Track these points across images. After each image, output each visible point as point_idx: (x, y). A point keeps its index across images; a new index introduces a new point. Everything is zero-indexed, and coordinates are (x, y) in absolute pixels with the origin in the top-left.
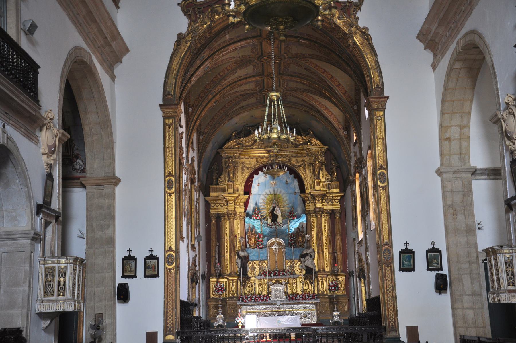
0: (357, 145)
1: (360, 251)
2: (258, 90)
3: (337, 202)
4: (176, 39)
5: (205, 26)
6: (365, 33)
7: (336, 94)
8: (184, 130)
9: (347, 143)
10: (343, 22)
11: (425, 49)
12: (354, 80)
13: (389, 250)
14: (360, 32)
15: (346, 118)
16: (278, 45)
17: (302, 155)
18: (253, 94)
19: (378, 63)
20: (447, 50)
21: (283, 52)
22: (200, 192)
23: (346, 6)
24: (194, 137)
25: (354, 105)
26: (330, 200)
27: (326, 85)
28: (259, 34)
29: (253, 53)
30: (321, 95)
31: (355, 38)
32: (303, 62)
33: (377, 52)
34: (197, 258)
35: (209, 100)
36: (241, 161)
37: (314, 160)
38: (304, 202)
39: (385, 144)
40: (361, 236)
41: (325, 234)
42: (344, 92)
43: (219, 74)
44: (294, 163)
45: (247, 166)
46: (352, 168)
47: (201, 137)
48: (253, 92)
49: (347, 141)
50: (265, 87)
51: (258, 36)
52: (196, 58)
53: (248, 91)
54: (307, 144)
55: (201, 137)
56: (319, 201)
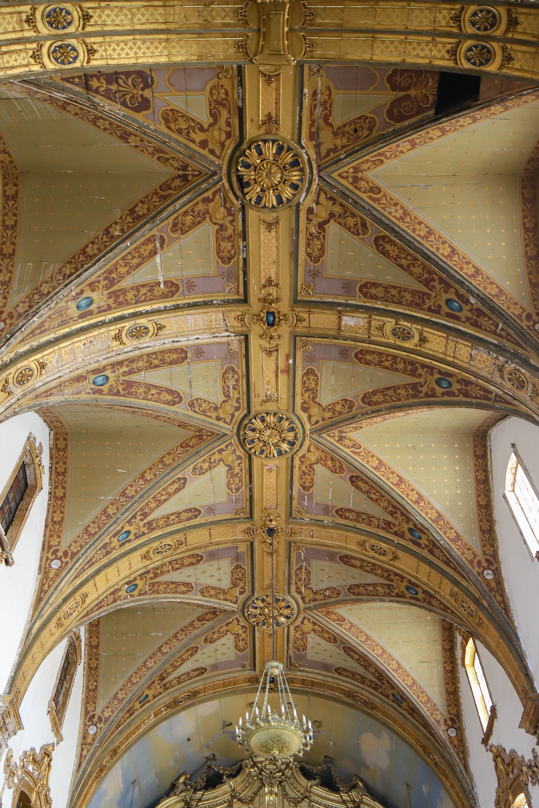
2: (242, 598)
9: (460, 759)
25: (485, 569)
32: (348, 451)
35: (112, 556)
42: (453, 535)
43: (142, 476)
49: (458, 754)
50: (257, 585)
51: (239, 301)
53: (216, 596)
55: (92, 730)
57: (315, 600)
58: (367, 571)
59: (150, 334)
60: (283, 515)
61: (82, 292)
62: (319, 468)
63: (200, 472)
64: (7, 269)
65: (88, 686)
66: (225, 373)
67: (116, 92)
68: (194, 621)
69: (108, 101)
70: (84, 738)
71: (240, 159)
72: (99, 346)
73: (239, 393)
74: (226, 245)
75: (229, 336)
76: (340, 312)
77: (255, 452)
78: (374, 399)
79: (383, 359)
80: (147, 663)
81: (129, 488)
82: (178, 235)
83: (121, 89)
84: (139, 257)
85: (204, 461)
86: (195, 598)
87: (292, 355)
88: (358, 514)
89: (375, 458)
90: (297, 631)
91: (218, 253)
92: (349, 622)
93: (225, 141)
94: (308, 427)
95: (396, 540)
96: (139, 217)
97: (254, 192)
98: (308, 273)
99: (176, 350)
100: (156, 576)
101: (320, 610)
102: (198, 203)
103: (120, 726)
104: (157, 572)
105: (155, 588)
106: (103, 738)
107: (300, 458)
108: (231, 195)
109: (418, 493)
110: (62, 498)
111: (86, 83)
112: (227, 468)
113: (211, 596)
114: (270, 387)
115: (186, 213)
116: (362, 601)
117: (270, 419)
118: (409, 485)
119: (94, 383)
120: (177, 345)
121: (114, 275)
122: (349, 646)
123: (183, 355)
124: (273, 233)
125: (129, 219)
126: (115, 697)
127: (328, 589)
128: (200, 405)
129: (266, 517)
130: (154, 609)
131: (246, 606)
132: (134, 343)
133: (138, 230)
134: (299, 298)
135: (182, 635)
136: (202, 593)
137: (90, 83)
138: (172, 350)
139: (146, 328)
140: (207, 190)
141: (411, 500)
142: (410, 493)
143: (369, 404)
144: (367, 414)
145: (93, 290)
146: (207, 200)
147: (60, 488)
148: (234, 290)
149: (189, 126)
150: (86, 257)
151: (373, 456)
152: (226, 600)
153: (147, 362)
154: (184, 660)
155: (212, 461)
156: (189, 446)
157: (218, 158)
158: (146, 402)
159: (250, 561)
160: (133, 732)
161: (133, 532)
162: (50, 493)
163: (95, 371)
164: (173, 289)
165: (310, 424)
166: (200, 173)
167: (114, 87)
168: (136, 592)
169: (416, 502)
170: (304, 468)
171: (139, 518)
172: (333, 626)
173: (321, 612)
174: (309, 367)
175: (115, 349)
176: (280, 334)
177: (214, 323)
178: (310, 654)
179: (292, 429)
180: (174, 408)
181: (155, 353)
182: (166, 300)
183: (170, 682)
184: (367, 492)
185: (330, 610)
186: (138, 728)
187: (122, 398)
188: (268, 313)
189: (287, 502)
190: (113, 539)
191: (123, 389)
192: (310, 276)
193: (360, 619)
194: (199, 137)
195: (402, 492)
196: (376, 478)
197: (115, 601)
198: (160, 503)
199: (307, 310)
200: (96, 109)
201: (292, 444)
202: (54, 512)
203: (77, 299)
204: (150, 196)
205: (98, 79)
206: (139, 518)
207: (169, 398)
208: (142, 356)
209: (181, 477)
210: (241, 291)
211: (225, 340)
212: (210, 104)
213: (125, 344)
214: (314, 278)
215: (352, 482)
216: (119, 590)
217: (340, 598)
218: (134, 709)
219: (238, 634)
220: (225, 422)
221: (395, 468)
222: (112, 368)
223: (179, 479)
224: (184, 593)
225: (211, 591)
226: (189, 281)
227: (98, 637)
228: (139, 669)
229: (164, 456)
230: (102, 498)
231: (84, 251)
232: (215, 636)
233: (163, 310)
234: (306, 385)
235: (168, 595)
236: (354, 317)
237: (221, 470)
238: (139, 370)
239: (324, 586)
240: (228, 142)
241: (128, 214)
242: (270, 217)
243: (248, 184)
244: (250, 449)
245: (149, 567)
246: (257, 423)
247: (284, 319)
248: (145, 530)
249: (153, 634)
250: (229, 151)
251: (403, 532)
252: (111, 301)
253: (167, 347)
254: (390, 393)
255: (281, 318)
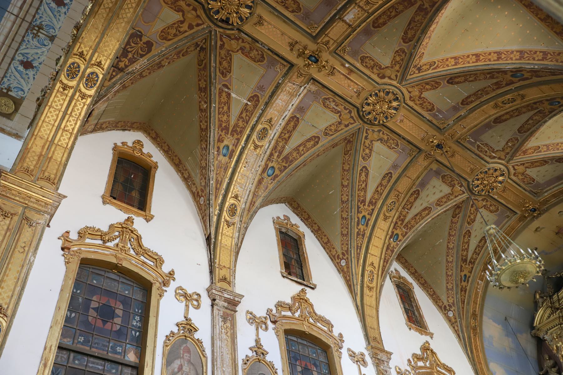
7: (535, 72)
27: (508, 77)
32: (430, 71)
42: (540, 56)
43: (343, 186)
47: (450, 314)
51: (290, 69)
53: (449, 200)
55: (451, 314)
57: (508, 153)
58: (517, 116)
59: (269, 128)
60: (435, 133)
61: (218, 148)
62: (425, 94)
63: (368, 157)
64: (184, 170)
65: (430, 294)
66: (324, 105)
67: (133, 56)
68: (452, 220)
69: (135, 64)
70: (450, 321)
71: (212, 14)
72: (252, 160)
73: (342, 105)
74: (254, 53)
75: (305, 87)
76: (340, 18)
77: (383, 121)
78: (409, 36)
79: (389, 13)
80: (448, 260)
81: (342, 197)
82: (229, 76)
83: (133, 52)
84: (225, 105)
85: (364, 150)
86: (440, 210)
87: (344, 62)
88: (475, 94)
89: (449, 60)
90: (518, 176)
91: (255, 61)
92: (544, 146)
93: (197, 13)
94: (395, 83)
95: (512, 87)
96: (205, 88)
97: (234, 18)
98: (303, 19)
99: (289, 121)
100: (403, 221)
101: (518, 155)
102: (220, 53)
103: (464, 302)
104: (401, 218)
105: (409, 226)
106: (459, 314)
107: (410, 100)
108: (228, 32)
109: (495, 53)
110: (319, 229)
111: (119, 69)
112: (379, 141)
113: (446, 202)
114: (352, 87)
115: (221, 63)
116: (534, 131)
117: (371, 100)
118: (485, 53)
119: (269, 176)
120: (287, 118)
121: (224, 125)
122: (557, 158)
123: (295, 119)
124: (265, 24)
125: (203, 94)
126: (448, 289)
127: (508, 142)
128: (330, 130)
129: (428, 143)
130: (425, 231)
131: (472, 189)
132: (266, 140)
133: (211, 95)
134: (314, 34)
135: (452, 232)
136: (439, 205)
137: (120, 67)
138: (288, 122)
139: (264, 128)
140: (216, 43)
141: (494, 60)
142: (490, 57)
143: (411, 41)
144: (416, 46)
145: (223, 141)
146: (222, 46)
147: (314, 225)
148: (282, 67)
149: (176, 28)
150: (205, 131)
151: (447, 60)
152: (456, 197)
153: (283, 140)
154: (468, 243)
155: (368, 146)
156: (349, 151)
157: (203, 24)
158: (303, 156)
159: (446, 169)
160: (476, 297)
161: (366, 214)
162: (312, 231)
163: (264, 171)
164: (255, 99)
165: (394, 80)
166: (205, 39)
167: (130, 55)
168: (400, 237)
170: (418, 102)
171: (362, 206)
172: (536, 156)
173: (520, 155)
174: (359, 57)
175: (261, 153)
176: (326, 60)
177: (291, 91)
178: (540, 179)
179: (388, 93)
180: (320, 144)
181: (282, 133)
182: (258, 107)
183: (472, 258)
184: (466, 80)
185: (524, 149)
186: (477, 293)
187: (289, 168)
188: (308, 58)
189: (430, 126)
190: (359, 228)
191: (286, 163)
192: (306, 19)
193: (549, 138)
194: (185, 27)
195: (485, 61)
196: (461, 70)
197: (392, 251)
198: (365, 189)
199: (324, 35)
200: (135, 73)
201: (397, 99)
202: (322, 238)
203: (220, 153)
204: (199, 74)
205: (121, 61)
206: (362, 206)
207: (312, 143)
208: (277, 141)
209: (361, 168)
210: (285, 63)
211: (305, 91)
212: (172, 8)
213: (263, 146)
214: (308, 18)
215: (452, 83)
216: (389, 244)
217: (520, 140)
218: (464, 287)
219: (484, 206)
220: (352, 124)
221: (466, 53)
222: (270, 161)
223: (362, 170)
224: (428, 214)
225: (443, 200)
226: (258, 87)
227: (412, 267)
228: (447, 266)
229: (343, 167)
230: (335, 213)
231: (202, 130)
232: (472, 217)
233: (262, 112)
234: (369, 66)
235: (421, 222)
236: (348, 13)
237: (377, 145)
238: (283, 147)
239: (503, 143)
240: (199, 13)
241: (200, 93)
242: (255, 19)
243: (228, 19)
244: (379, 122)
245: (394, 220)
246: (367, 108)
247: (319, 52)
248: (371, 207)
249: (437, 243)
250: (204, 15)
251: (510, 80)
252: (236, 136)
253: (283, 124)
254: (412, 25)
255: (317, 53)
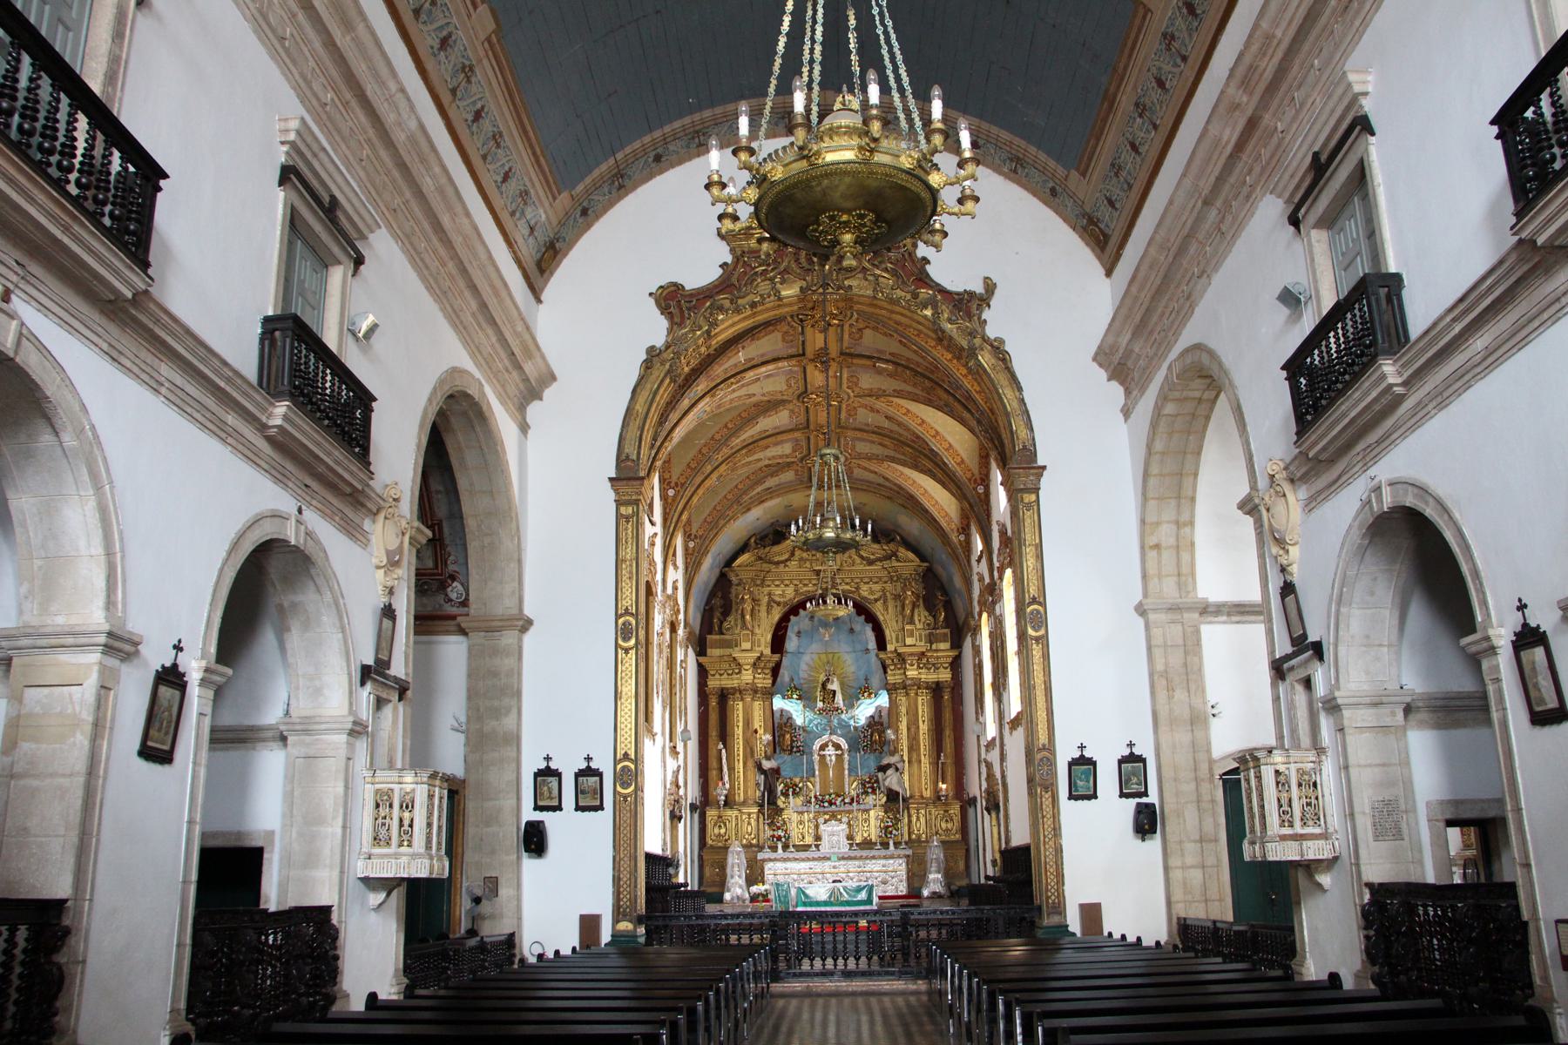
0: (984, 561)
1: (989, 760)
2: (799, 456)
3: (946, 668)
4: (644, 357)
5: (698, 333)
6: (998, 348)
7: (945, 464)
8: (658, 529)
10: (958, 328)
11: (1109, 380)
12: (978, 437)
13: (1048, 759)
14: (989, 348)
15: (962, 509)
16: (836, 372)
17: (880, 578)
18: (789, 465)
19: (1025, 404)
20: (1151, 381)
21: (845, 386)
22: (687, 647)
23: (962, 299)
24: (679, 541)
26: (934, 665)
28: (801, 352)
29: (790, 386)
30: (916, 467)
31: (980, 358)
33: (1022, 385)
34: (681, 772)
36: (766, 590)
37: (902, 588)
38: (885, 668)
39: (1040, 556)
40: (991, 731)
41: (924, 728)
43: (726, 426)
44: (865, 594)
45: (777, 599)
46: (975, 603)
48: (788, 460)
50: (812, 451)
51: (799, 355)
52: (683, 395)
54: (890, 558)
55: (691, 544)
56: (913, 665)
126: (705, 521)
169: (934, 437)
